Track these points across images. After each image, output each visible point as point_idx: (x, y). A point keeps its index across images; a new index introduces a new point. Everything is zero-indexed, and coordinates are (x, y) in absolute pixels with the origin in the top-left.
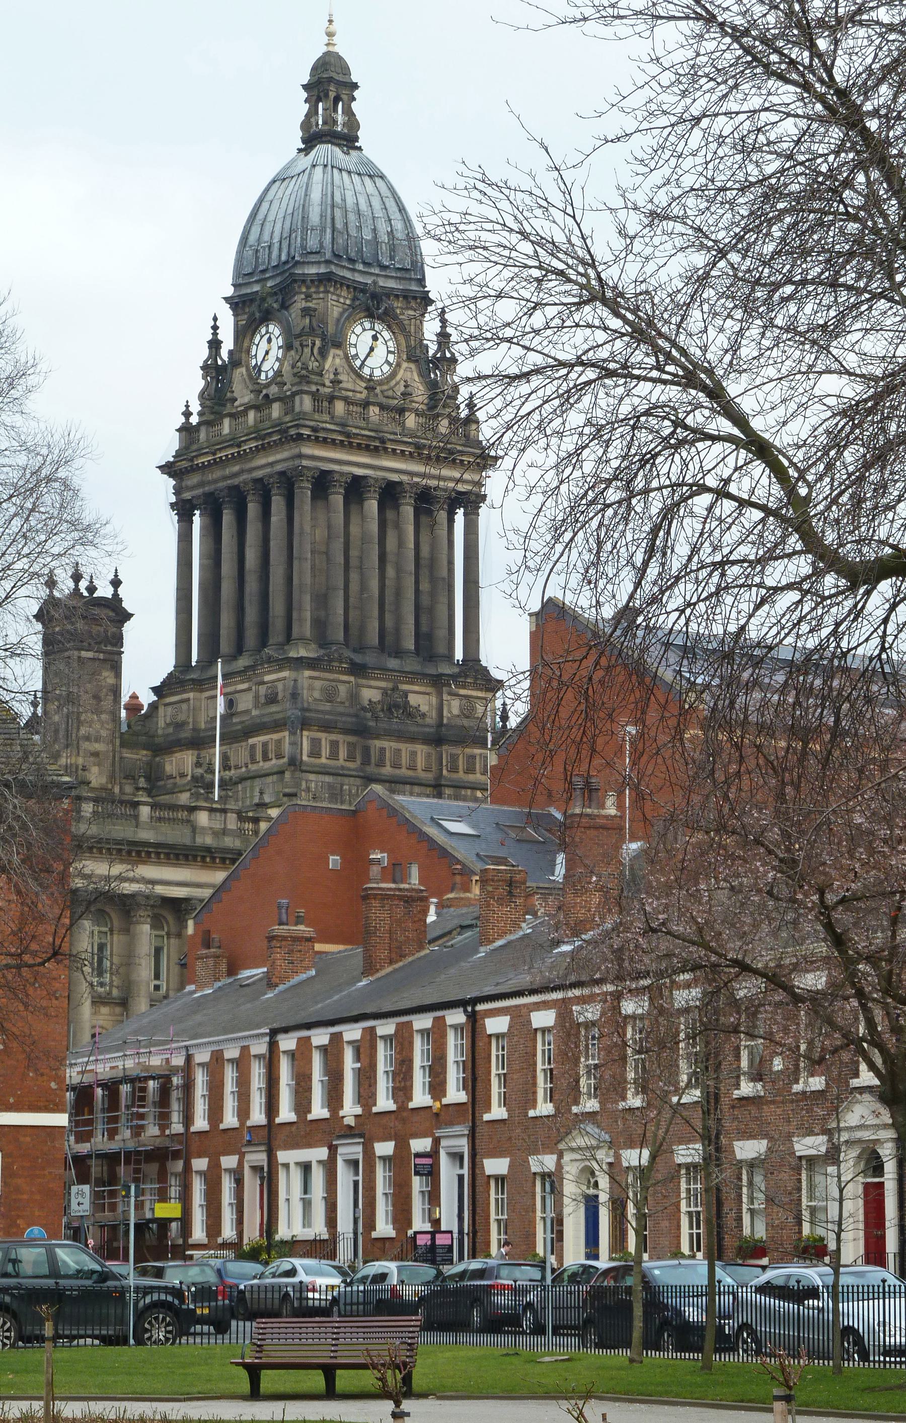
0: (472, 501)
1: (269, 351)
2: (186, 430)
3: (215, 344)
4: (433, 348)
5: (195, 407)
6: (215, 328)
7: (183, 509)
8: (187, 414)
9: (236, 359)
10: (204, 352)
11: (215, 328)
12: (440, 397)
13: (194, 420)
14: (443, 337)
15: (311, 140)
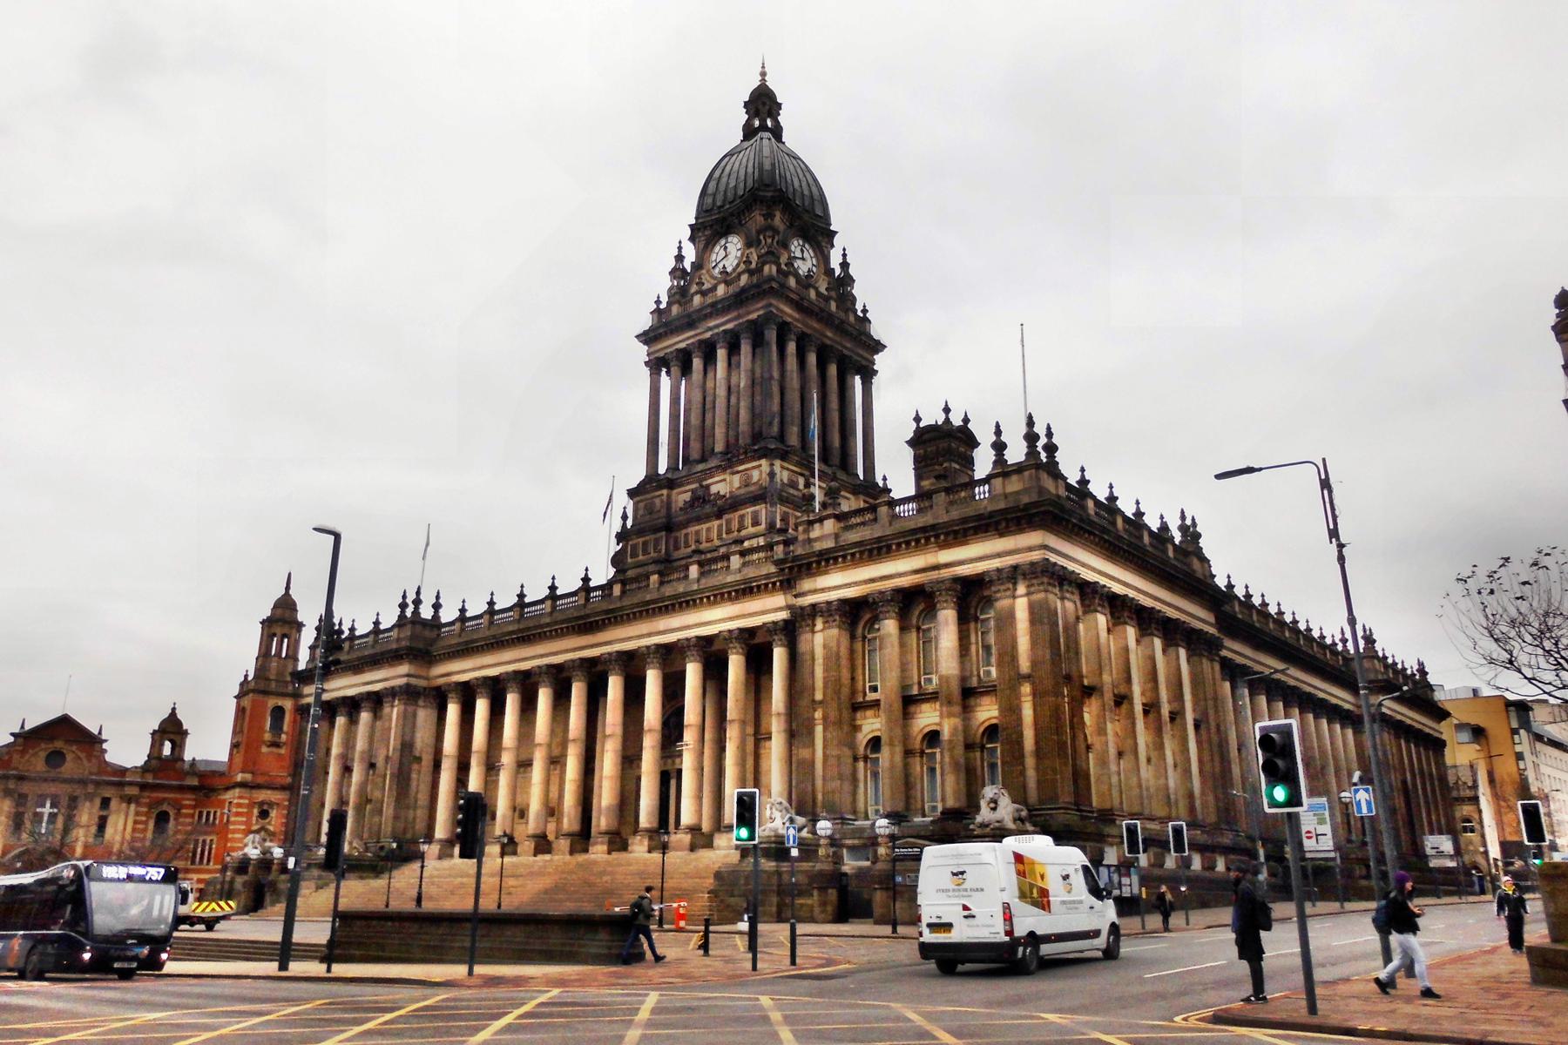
0: (868, 374)
1: (730, 253)
2: (658, 312)
3: (680, 258)
4: (838, 272)
5: (665, 300)
6: (680, 248)
7: (656, 365)
8: (658, 302)
9: (698, 266)
10: (672, 263)
11: (680, 248)
12: (847, 300)
13: (663, 306)
14: (845, 265)
15: (749, 132)
